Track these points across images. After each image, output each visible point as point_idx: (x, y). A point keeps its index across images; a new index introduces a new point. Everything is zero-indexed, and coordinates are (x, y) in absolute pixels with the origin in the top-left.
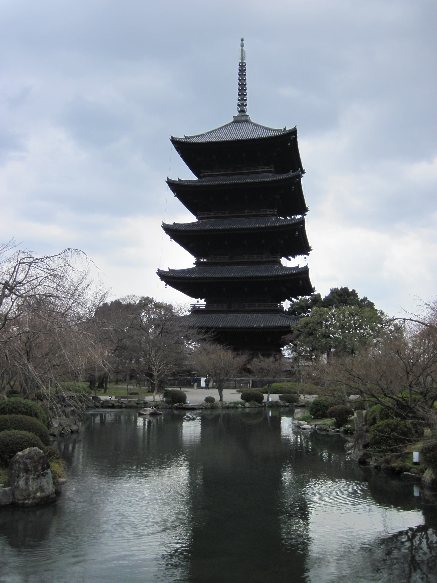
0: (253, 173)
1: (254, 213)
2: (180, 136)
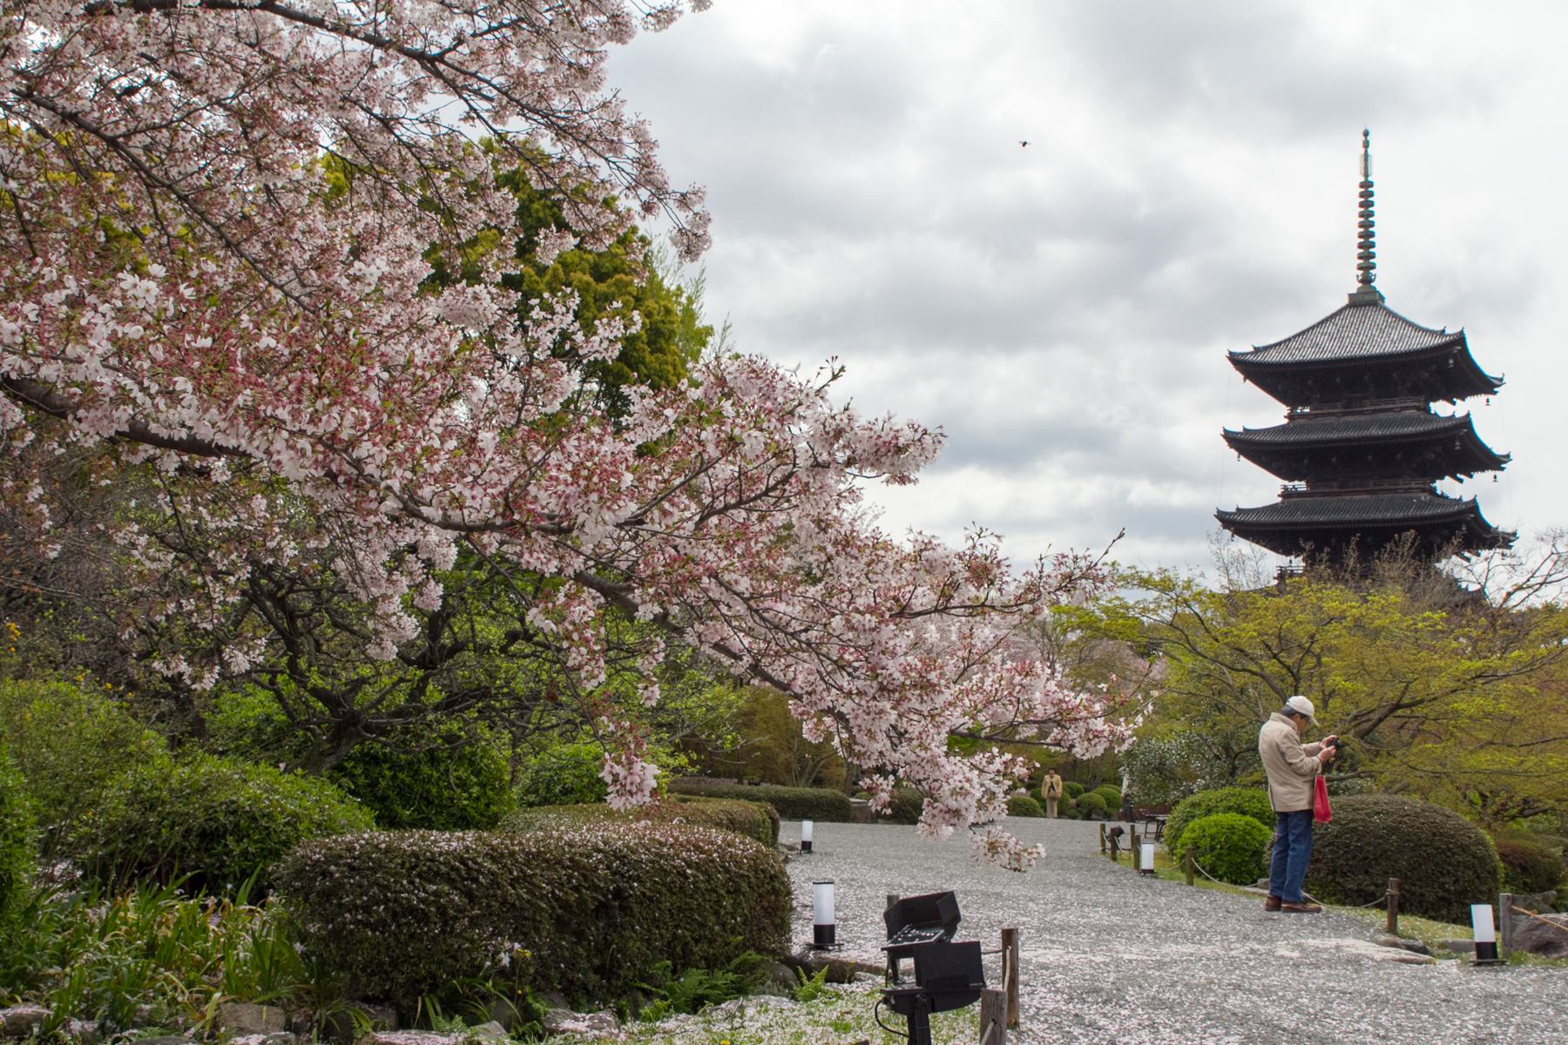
1: (1386, 486)
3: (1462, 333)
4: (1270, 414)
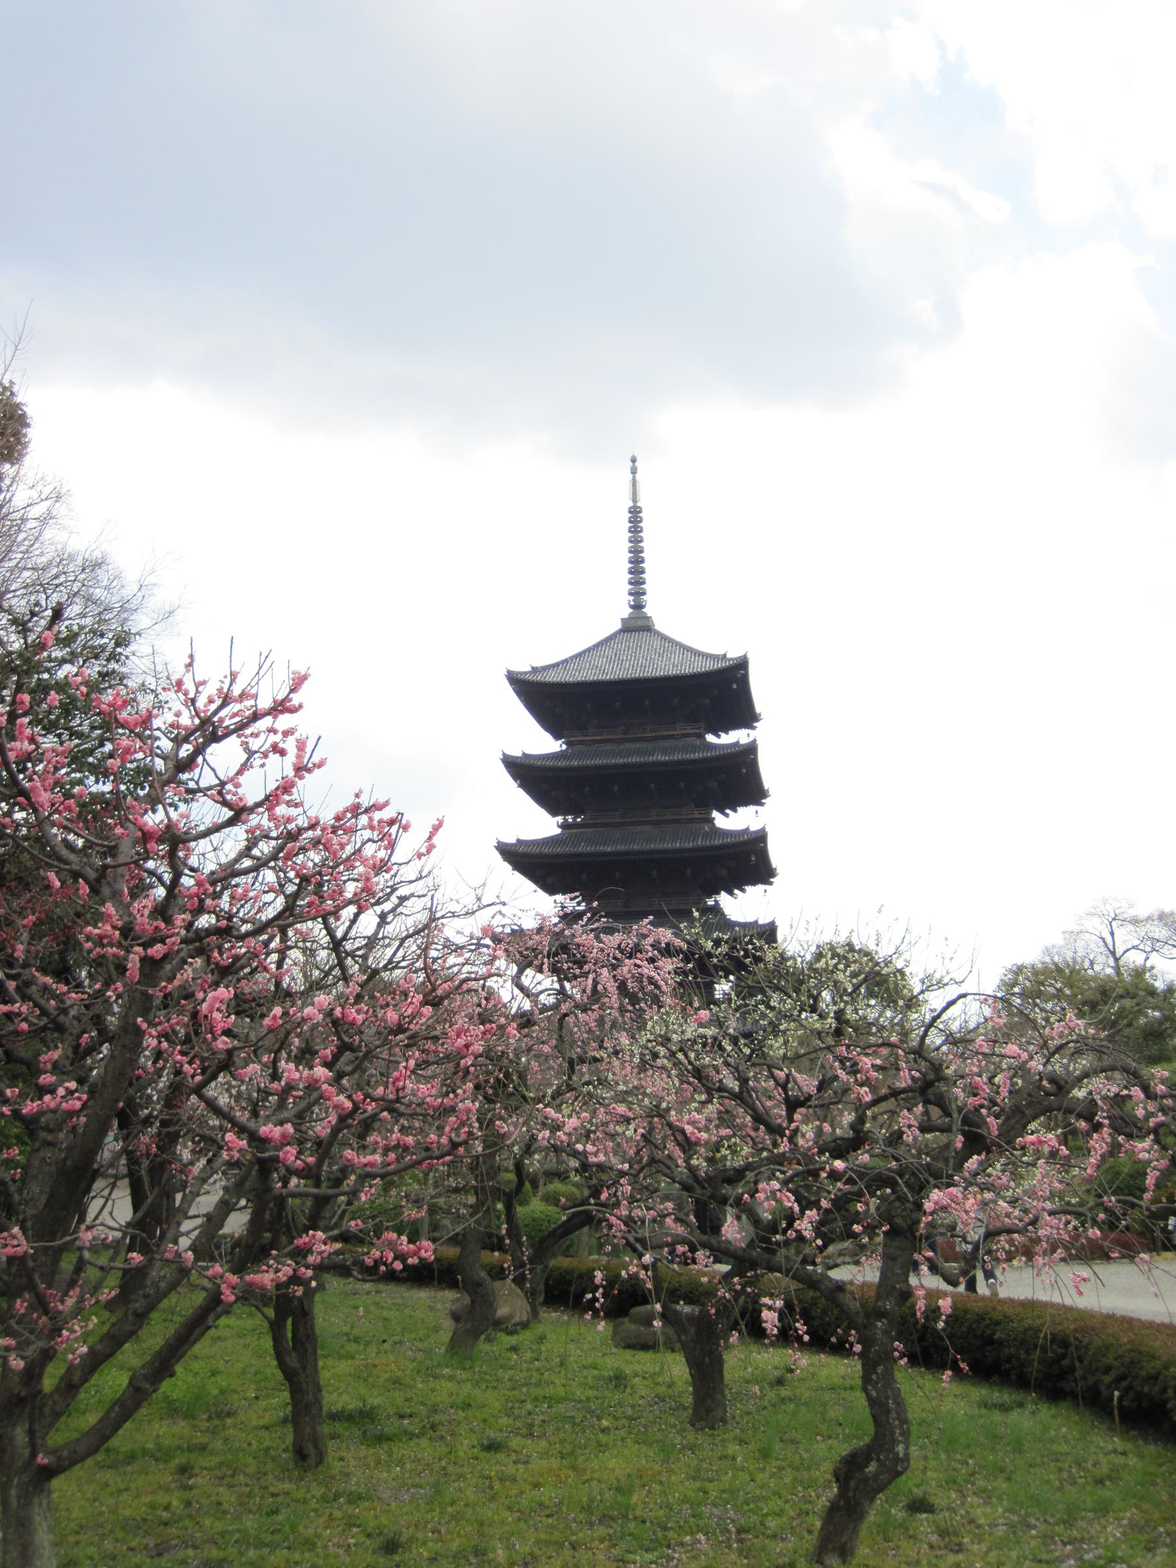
0: (664, 738)
1: (668, 817)
2: (522, 666)
3: (745, 656)
4: (542, 743)
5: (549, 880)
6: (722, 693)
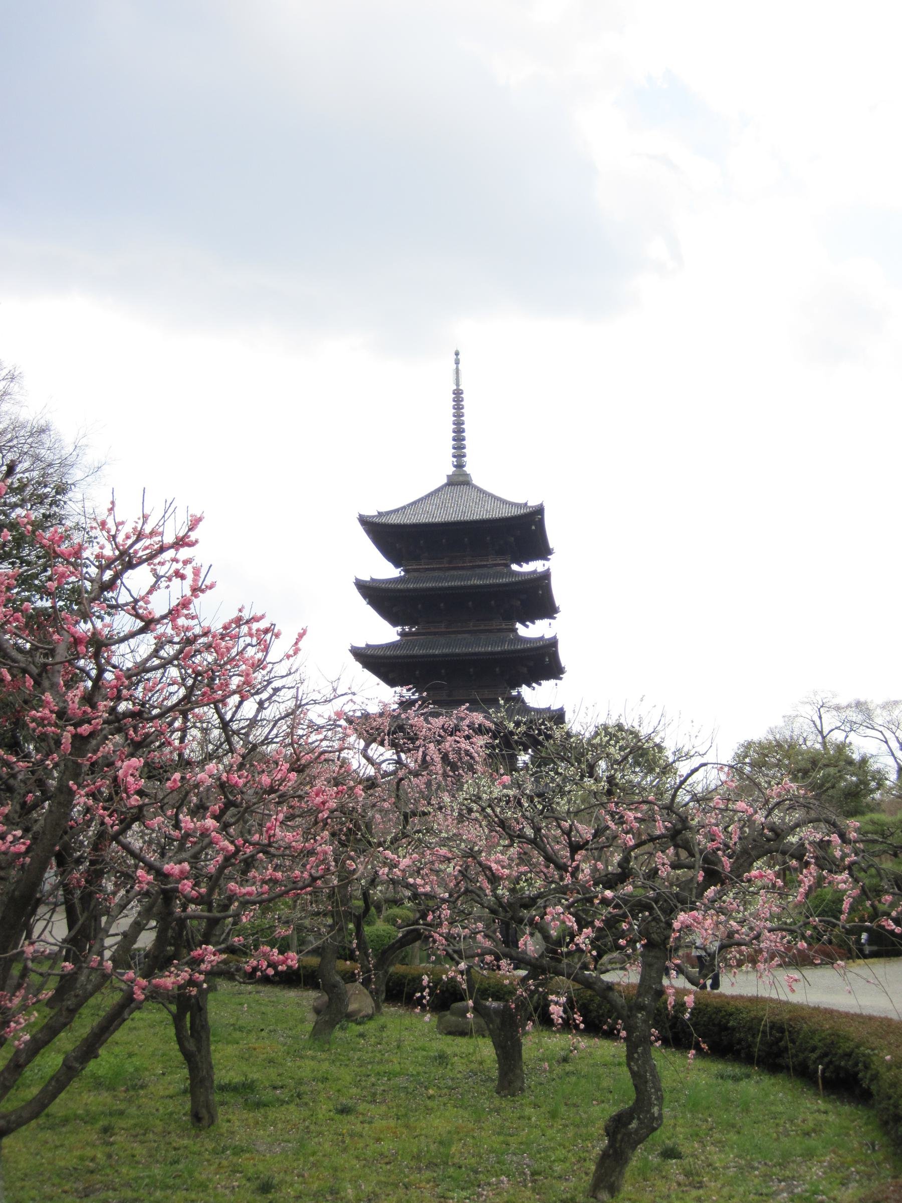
2: (370, 511)
3: (542, 505)
4: (385, 570)
5: (390, 676)
6: (524, 532)
